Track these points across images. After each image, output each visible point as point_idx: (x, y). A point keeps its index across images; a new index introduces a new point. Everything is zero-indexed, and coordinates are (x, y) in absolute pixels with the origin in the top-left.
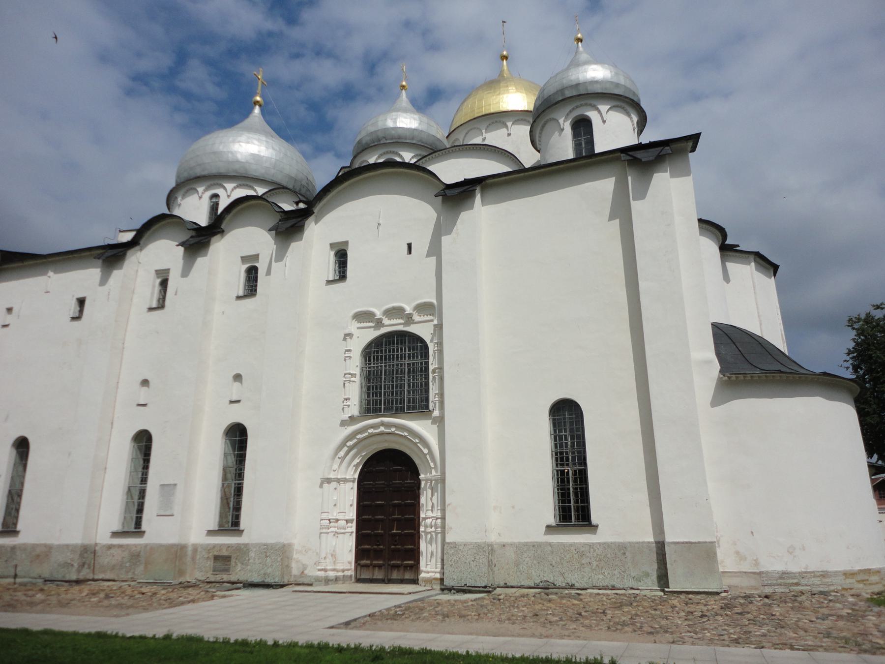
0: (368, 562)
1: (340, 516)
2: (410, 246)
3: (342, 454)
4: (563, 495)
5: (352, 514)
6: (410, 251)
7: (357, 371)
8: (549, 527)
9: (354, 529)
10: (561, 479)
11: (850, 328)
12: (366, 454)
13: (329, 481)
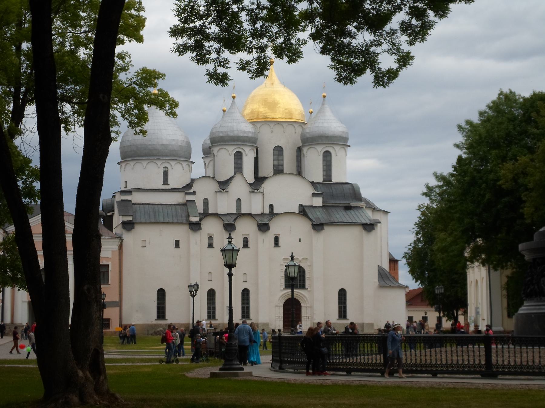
0: (287, 328)
1: (280, 316)
2: (300, 239)
3: (280, 299)
4: (340, 312)
5: (282, 316)
6: (300, 241)
7: (284, 276)
8: (337, 319)
9: (283, 319)
10: (340, 308)
11: (419, 211)
12: (286, 299)
13: (278, 306)
